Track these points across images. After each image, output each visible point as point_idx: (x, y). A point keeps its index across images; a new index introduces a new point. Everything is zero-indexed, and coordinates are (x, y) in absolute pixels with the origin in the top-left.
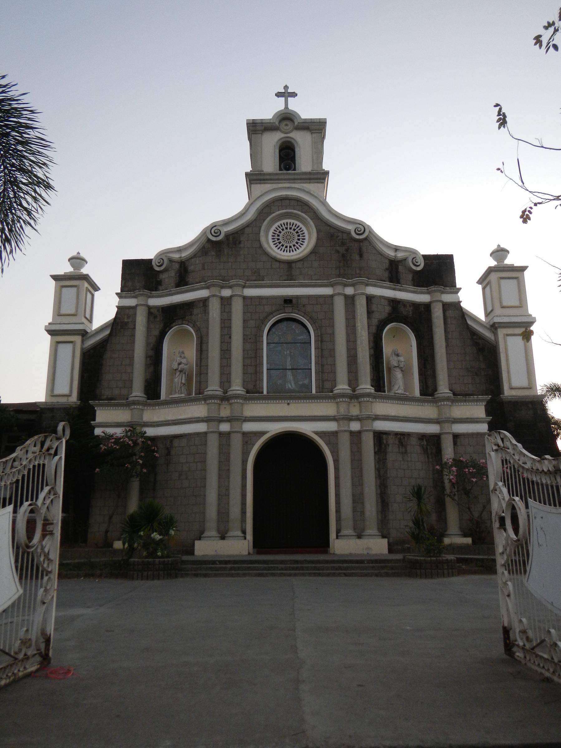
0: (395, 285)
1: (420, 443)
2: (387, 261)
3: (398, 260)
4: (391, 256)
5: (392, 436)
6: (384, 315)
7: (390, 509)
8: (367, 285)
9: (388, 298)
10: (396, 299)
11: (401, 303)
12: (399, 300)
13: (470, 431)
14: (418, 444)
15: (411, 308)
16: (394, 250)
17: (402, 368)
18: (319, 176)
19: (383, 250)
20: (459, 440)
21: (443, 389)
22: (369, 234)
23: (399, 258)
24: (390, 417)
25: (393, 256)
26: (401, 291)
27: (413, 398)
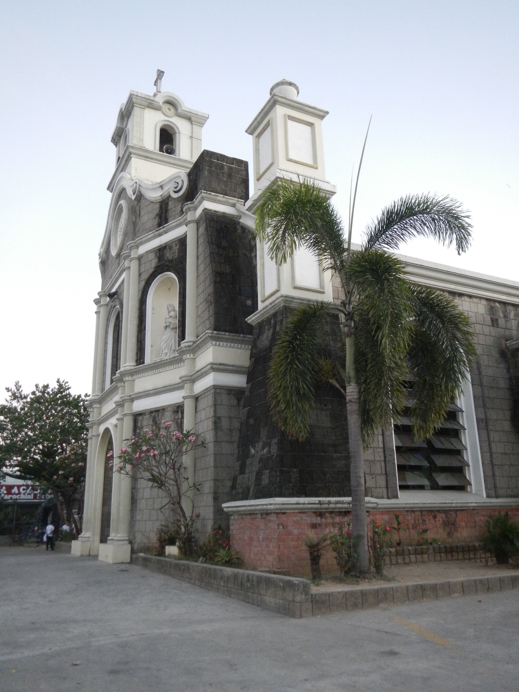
0: (157, 230)
1: (174, 418)
2: (158, 204)
3: (166, 197)
4: (157, 197)
5: (147, 416)
6: (151, 271)
7: (138, 508)
8: (137, 247)
9: (154, 250)
10: (161, 245)
11: (167, 247)
12: (164, 245)
13: (204, 388)
14: (172, 419)
15: (178, 247)
16: (160, 188)
17: (169, 326)
18: (127, 153)
19: (150, 197)
20: (198, 403)
21: (189, 336)
22: (139, 188)
23: (165, 194)
24: (142, 394)
25: (159, 197)
26: (168, 232)
27: (163, 362)
